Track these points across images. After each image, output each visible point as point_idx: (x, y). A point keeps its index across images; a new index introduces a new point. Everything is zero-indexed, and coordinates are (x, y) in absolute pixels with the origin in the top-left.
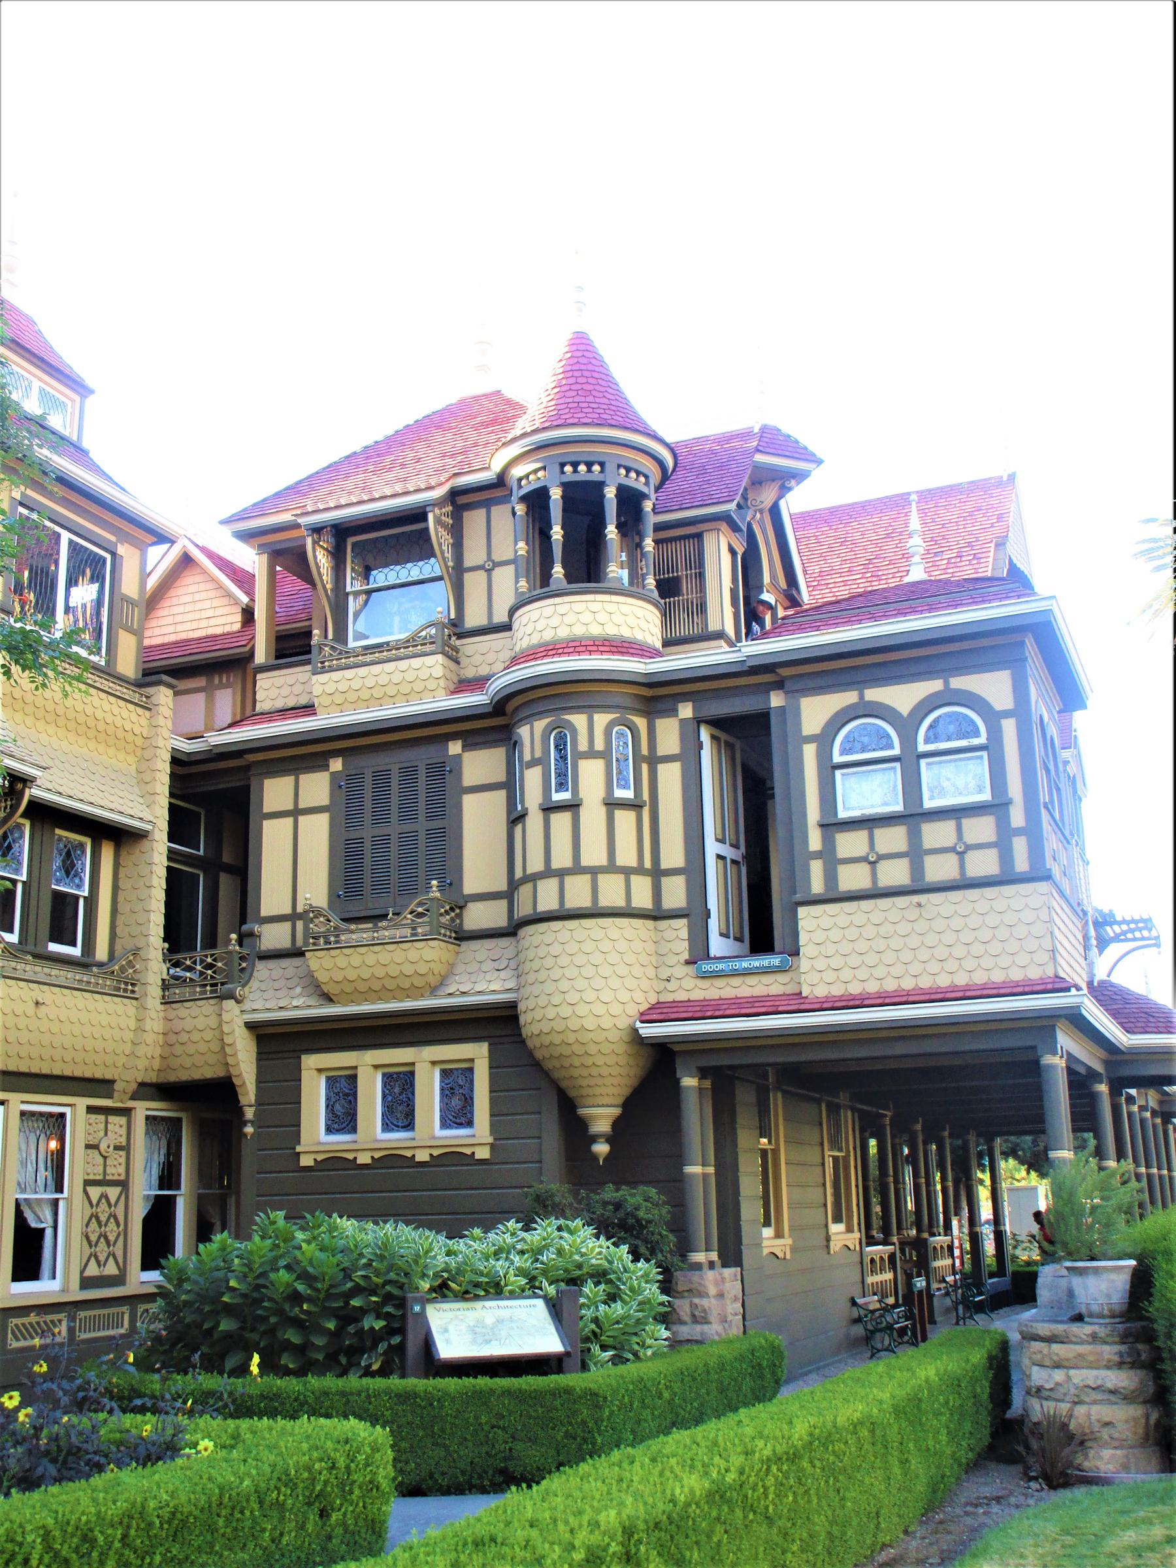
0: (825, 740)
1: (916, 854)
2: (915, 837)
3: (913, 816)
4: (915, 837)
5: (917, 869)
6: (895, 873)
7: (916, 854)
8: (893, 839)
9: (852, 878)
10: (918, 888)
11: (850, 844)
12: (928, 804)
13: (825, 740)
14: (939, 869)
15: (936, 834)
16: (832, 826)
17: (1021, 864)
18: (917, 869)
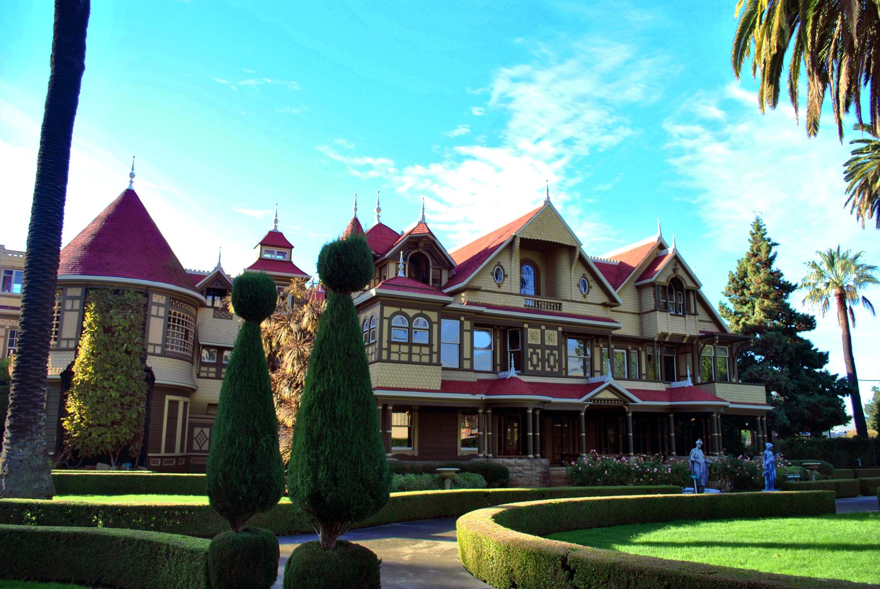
0: (390, 319)
1: (410, 354)
2: (410, 350)
3: (410, 344)
4: (410, 350)
5: (410, 357)
6: (405, 358)
7: (410, 354)
8: (405, 349)
9: (394, 357)
10: (410, 362)
11: (394, 348)
12: (414, 341)
13: (390, 319)
14: (415, 358)
15: (415, 350)
16: (390, 342)
17: (435, 360)
18: (410, 357)
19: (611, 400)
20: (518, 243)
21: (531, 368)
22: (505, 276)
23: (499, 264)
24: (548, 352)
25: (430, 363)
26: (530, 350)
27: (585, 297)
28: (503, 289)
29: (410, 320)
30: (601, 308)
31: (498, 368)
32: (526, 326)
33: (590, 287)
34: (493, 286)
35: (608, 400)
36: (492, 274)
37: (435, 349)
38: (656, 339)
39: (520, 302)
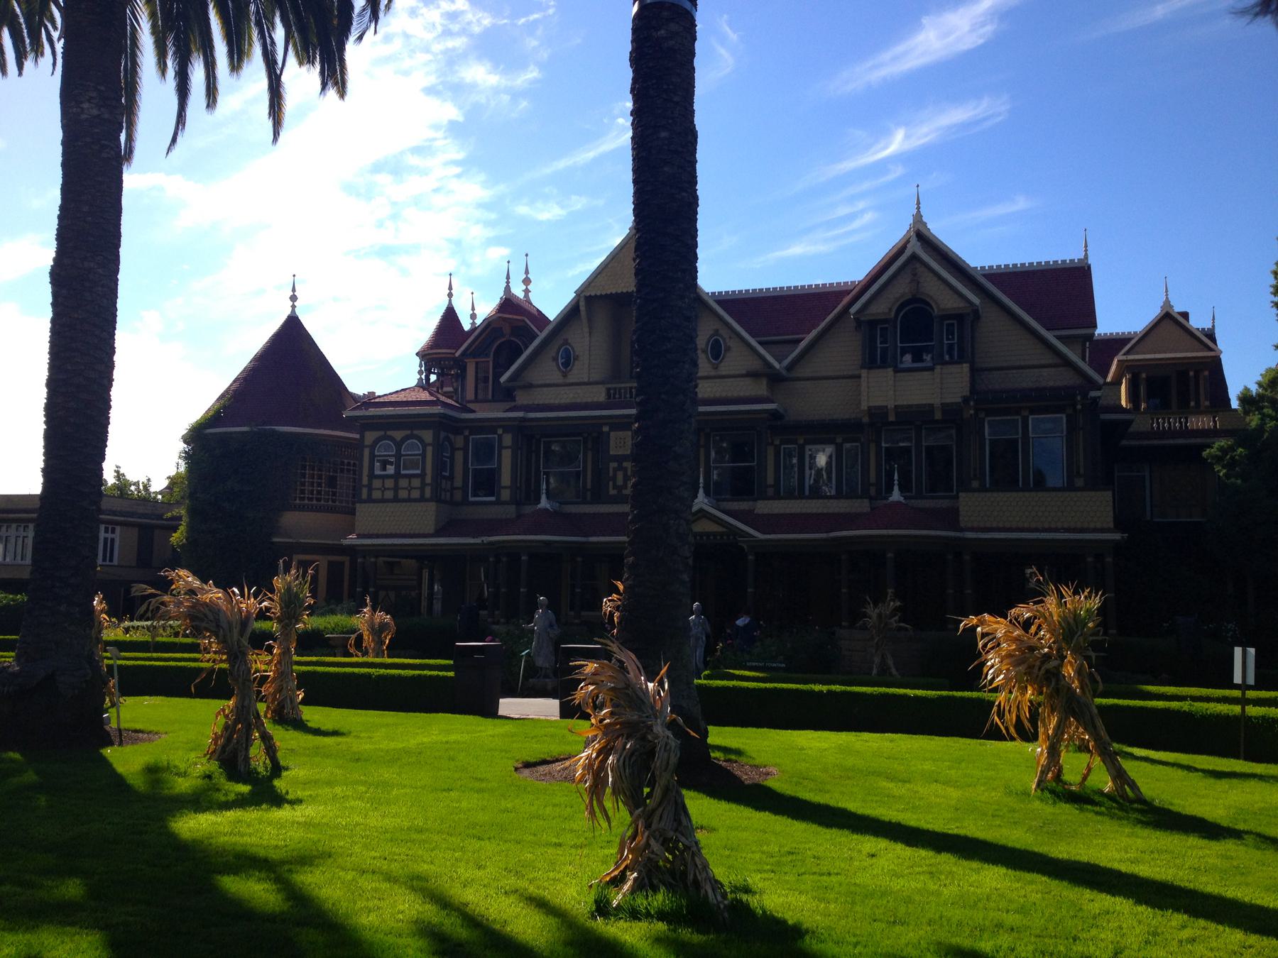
0: (373, 447)
1: (396, 489)
2: (396, 483)
4: (396, 483)
6: (389, 495)
7: (396, 489)
9: (377, 495)
10: (396, 499)
13: (373, 447)
19: (715, 534)
20: (582, 304)
21: (612, 492)
22: (576, 358)
23: (566, 342)
24: (613, 465)
25: (422, 499)
26: (613, 465)
27: (716, 368)
28: (571, 379)
29: (399, 445)
30: (748, 380)
31: (589, 494)
32: (606, 429)
33: (728, 349)
34: (556, 377)
35: (708, 534)
36: (555, 359)
37: (428, 479)
38: (866, 420)
39: (599, 394)
